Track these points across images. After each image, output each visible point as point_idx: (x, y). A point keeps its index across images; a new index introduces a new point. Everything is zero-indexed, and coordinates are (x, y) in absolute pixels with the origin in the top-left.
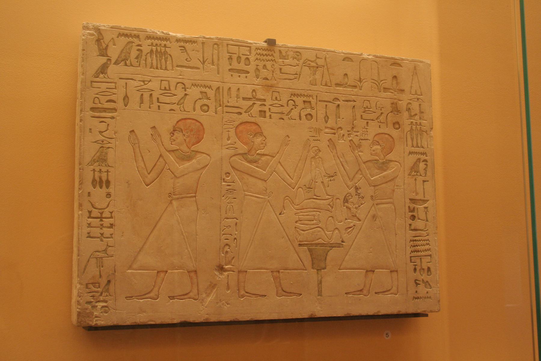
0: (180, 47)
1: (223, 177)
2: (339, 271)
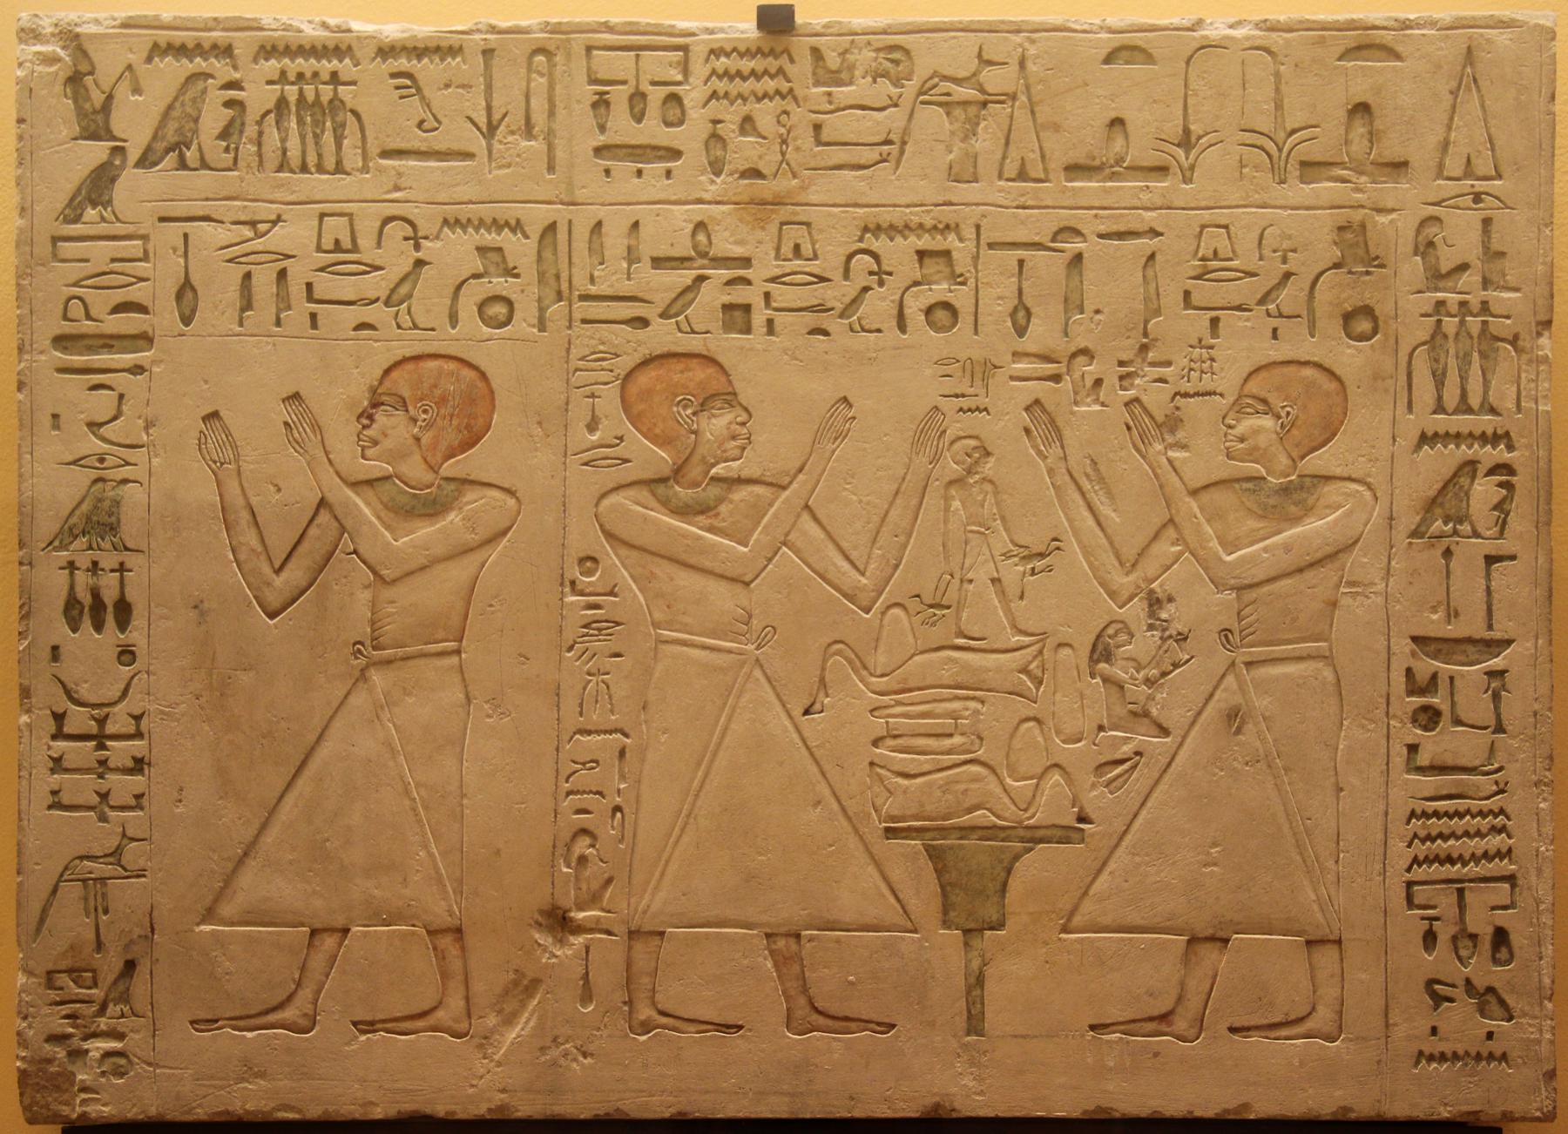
0: (394, 75)
1: (568, 576)
2: (1063, 936)
